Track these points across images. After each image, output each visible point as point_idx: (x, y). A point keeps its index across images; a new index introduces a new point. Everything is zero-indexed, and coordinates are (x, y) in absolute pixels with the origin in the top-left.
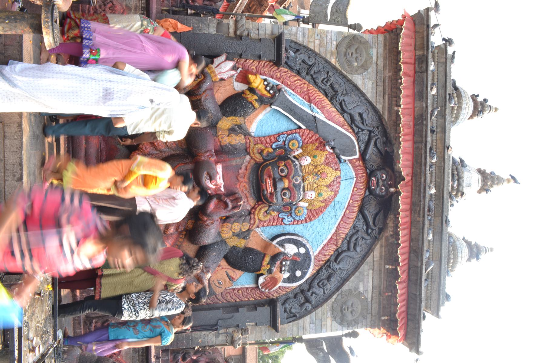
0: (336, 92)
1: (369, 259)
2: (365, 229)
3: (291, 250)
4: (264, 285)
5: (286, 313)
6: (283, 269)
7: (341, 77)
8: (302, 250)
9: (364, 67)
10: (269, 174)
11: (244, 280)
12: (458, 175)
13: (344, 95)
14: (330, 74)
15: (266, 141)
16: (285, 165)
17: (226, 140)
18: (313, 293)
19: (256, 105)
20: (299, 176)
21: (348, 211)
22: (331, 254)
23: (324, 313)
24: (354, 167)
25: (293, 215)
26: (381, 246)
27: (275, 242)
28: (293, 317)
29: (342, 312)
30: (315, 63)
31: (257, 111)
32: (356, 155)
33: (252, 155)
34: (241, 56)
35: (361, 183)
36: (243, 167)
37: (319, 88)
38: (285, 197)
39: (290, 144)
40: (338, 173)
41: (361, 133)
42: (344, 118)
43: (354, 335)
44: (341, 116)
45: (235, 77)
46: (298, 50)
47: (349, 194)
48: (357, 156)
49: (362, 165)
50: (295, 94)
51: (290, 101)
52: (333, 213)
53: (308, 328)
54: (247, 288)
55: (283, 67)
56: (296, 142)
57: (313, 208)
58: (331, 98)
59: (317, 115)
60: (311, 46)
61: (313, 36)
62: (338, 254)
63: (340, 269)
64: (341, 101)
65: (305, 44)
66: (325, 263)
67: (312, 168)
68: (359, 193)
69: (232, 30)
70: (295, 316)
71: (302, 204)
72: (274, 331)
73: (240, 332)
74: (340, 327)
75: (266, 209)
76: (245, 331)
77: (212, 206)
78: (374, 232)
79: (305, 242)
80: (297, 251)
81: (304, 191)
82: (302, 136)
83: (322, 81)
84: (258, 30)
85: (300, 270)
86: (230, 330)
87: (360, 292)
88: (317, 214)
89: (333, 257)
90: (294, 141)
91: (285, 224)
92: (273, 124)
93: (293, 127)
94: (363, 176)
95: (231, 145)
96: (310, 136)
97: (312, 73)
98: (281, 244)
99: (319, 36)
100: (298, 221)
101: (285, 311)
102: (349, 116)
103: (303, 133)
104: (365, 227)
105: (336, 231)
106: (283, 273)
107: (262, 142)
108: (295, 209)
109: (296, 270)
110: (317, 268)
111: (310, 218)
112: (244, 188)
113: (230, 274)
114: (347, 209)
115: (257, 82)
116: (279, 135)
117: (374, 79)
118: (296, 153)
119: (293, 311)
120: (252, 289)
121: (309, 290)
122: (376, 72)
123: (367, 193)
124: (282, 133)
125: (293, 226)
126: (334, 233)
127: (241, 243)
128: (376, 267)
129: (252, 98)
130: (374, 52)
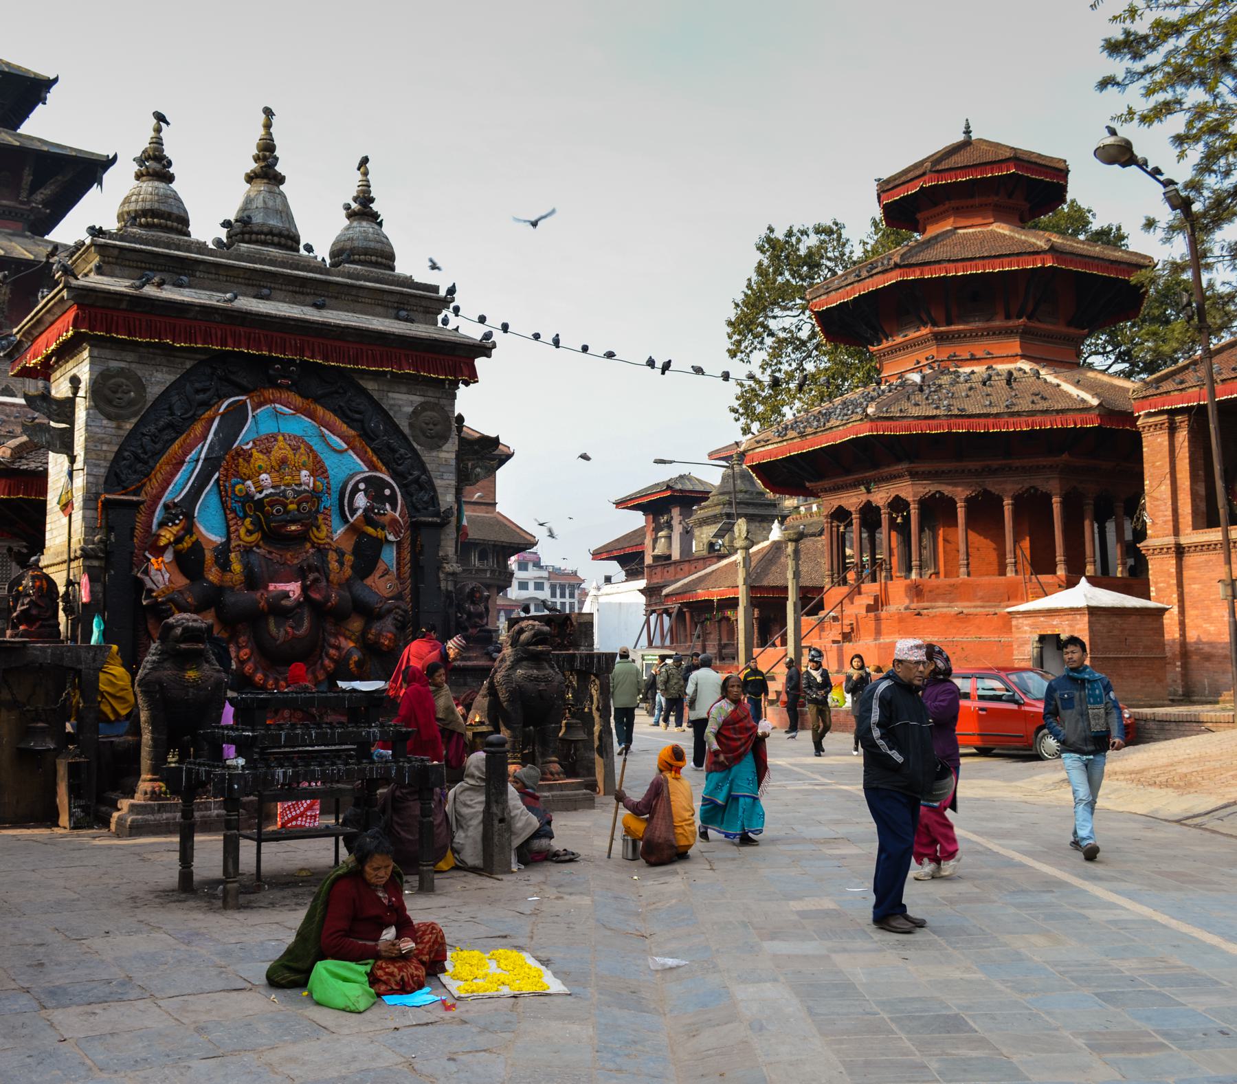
0: (170, 425)
1: (376, 396)
3: (361, 501)
4: (396, 534)
8: (362, 486)
10: (280, 527)
11: (389, 556)
12: (266, 235)
13: (172, 414)
16: (271, 507)
24: (260, 405)
26: (362, 379)
27: (351, 520)
29: (432, 437)
32: (245, 402)
34: (132, 553)
40: (280, 438)
43: (460, 419)
46: (116, 475)
56: (238, 487)
59: (203, 456)
60: (111, 456)
62: (367, 436)
67: (274, 474)
69: (96, 563)
76: (445, 559)
77: (316, 596)
79: (352, 483)
84: (94, 529)
86: (442, 576)
87: (413, 412)
93: (215, 489)
98: (353, 511)
107: (237, 530)
112: (294, 558)
115: (167, 535)
118: (253, 489)
119: (425, 499)
121: (406, 478)
127: (349, 558)
128: (385, 388)
129: (186, 544)
130: (114, 364)
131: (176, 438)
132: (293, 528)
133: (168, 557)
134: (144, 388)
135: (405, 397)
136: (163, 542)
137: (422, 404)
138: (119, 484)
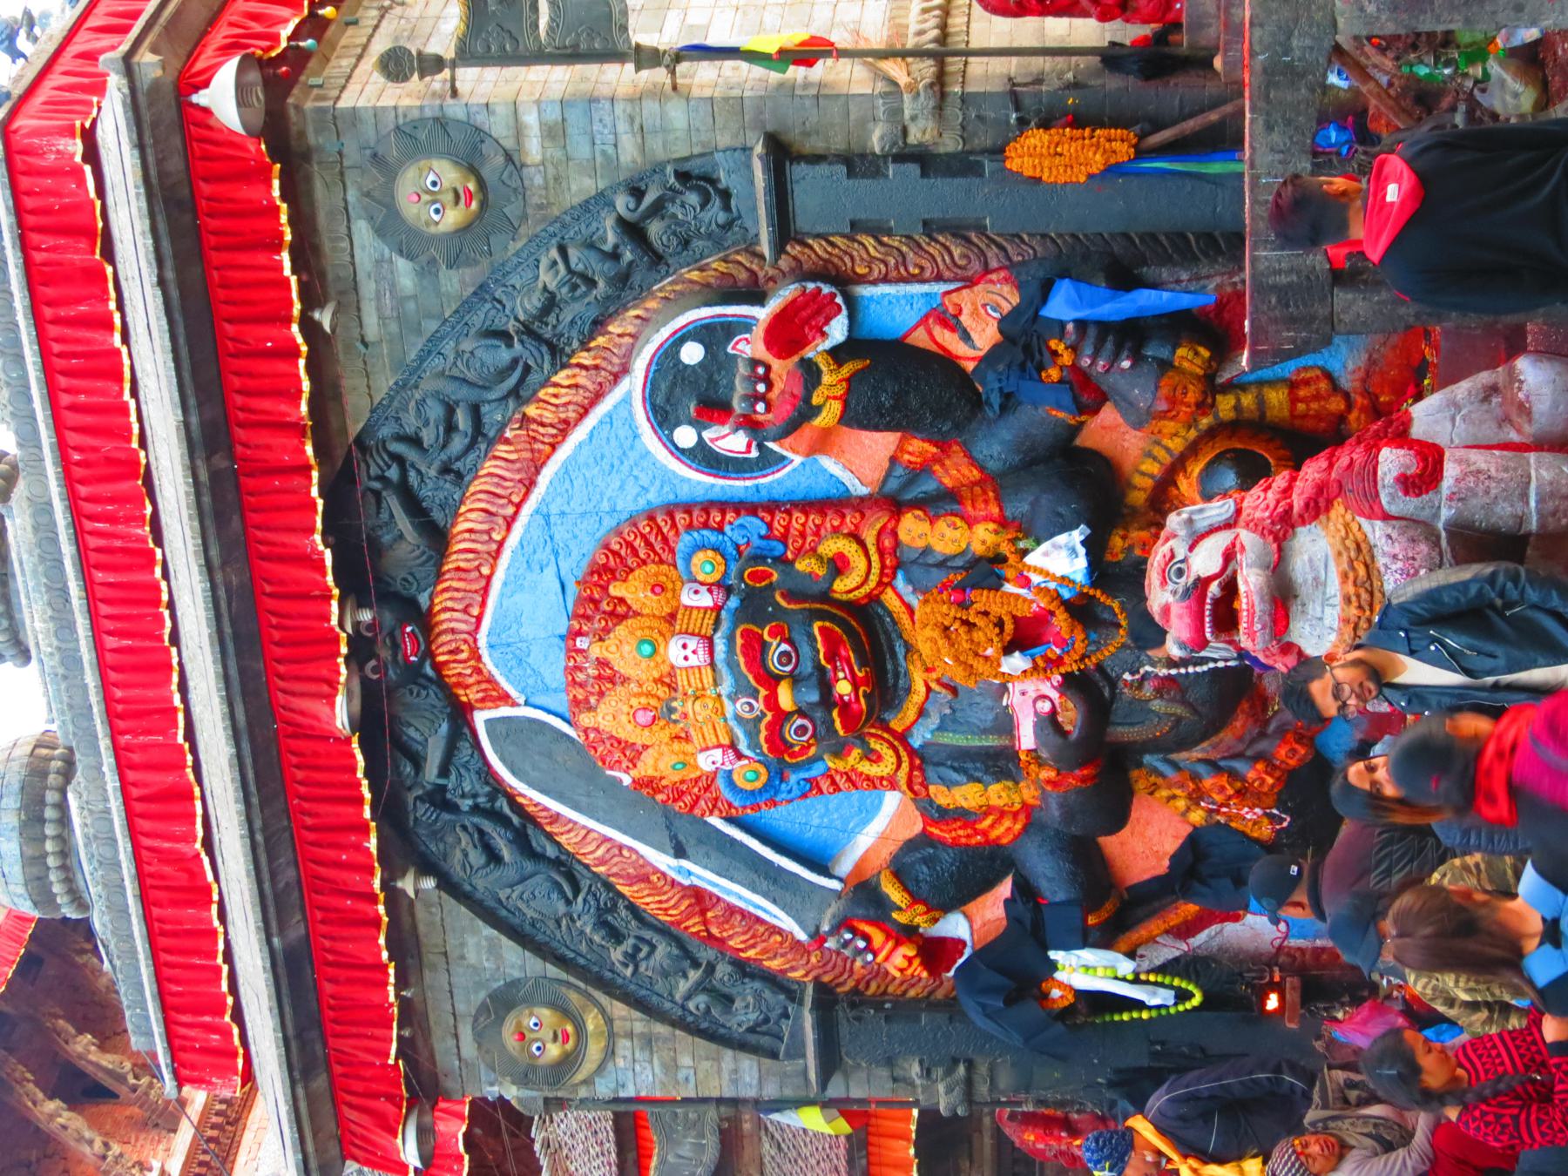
2: (412, 474)
3: (734, 442)
5: (722, 186)
6: (761, 388)
7: (582, 961)
8: (686, 436)
9: (504, 1001)
14: (629, 972)
15: (849, 779)
17: (998, 793)
18: (615, 256)
19: (895, 894)
20: (738, 718)
21: (497, 537)
22: (551, 390)
23: (556, 179)
25: (731, 550)
26: (344, 430)
28: (695, 178)
30: (688, 997)
31: (886, 854)
32: (488, 722)
33: (901, 749)
35: (453, 631)
36: (934, 721)
37: (663, 931)
38: (785, 647)
39: (764, 778)
41: (481, 800)
42: (558, 844)
44: (570, 849)
45: (967, 952)
46: (751, 1030)
47: (502, 595)
48: (480, 718)
49: (461, 692)
50: (751, 909)
51: (774, 901)
52: (560, 533)
53: (622, 127)
54: (885, 279)
55: (798, 983)
57: (652, 568)
58: (615, 905)
61: (701, 1075)
63: (505, 336)
64: (576, 897)
65: (728, 1054)
66: (570, 357)
68: (456, 594)
69: (983, 1069)
70: (683, 176)
71: (706, 600)
72: (769, 128)
73: (912, 140)
74: (480, 119)
75: (841, 586)
78: (374, 471)
80: (706, 435)
81: (712, 664)
82: (716, 799)
83: (653, 948)
85: (686, 366)
87: (410, 257)
88: (629, 545)
89: (534, 378)
90: (749, 787)
91: (751, 509)
92: (821, 817)
94: (451, 652)
95: (979, 781)
96: (688, 799)
97: (694, 975)
99: (681, 1075)
100: (706, 525)
101: (726, 195)
102: (539, 849)
103: (714, 806)
104: (413, 477)
105: (538, 472)
106: (761, 371)
108: (725, 574)
109: (701, 364)
110: (601, 340)
111: (660, 529)
113: (956, 336)
114: (501, 544)
115: (899, 960)
116: (804, 796)
117: (457, 970)
119: (693, 198)
120: (862, 280)
121: (631, 263)
122: (455, 991)
123: (423, 600)
124: (790, 801)
125: (715, 495)
126: (544, 463)
130: (469, 1048)
131: (633, 908)
132: (843, 688)
133: (955, 926)
134: (514, 984)
135: (368, 288)
136: (917, 969)
137: (380, 232)
138: (777, 1023)
